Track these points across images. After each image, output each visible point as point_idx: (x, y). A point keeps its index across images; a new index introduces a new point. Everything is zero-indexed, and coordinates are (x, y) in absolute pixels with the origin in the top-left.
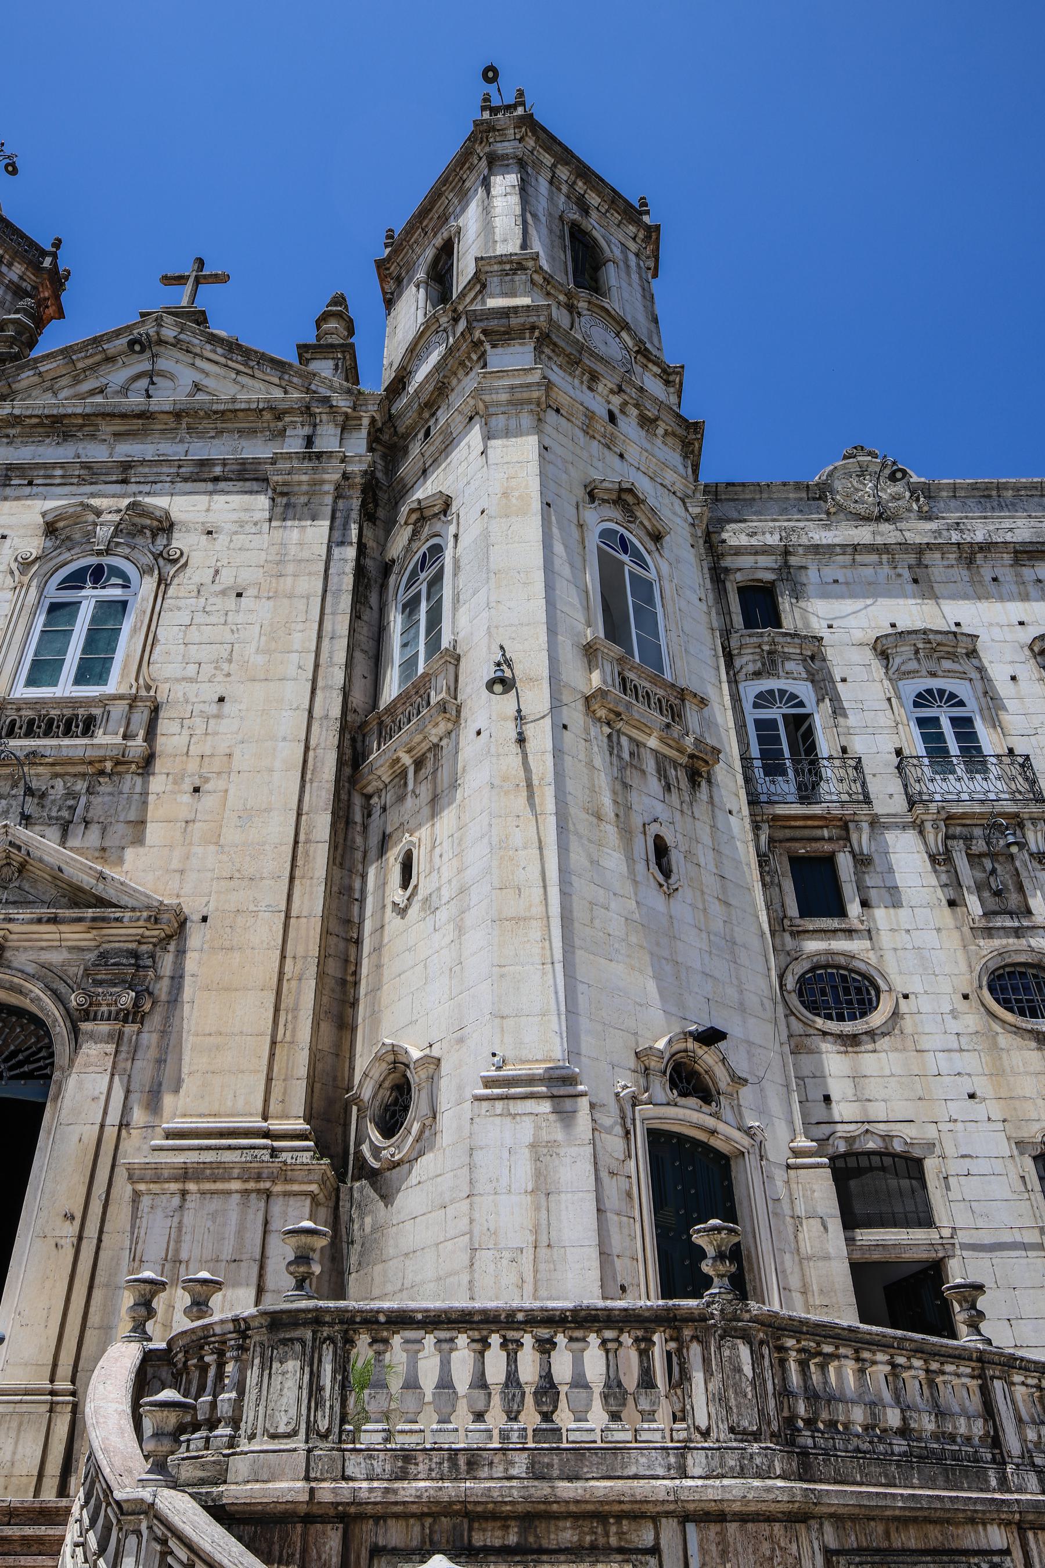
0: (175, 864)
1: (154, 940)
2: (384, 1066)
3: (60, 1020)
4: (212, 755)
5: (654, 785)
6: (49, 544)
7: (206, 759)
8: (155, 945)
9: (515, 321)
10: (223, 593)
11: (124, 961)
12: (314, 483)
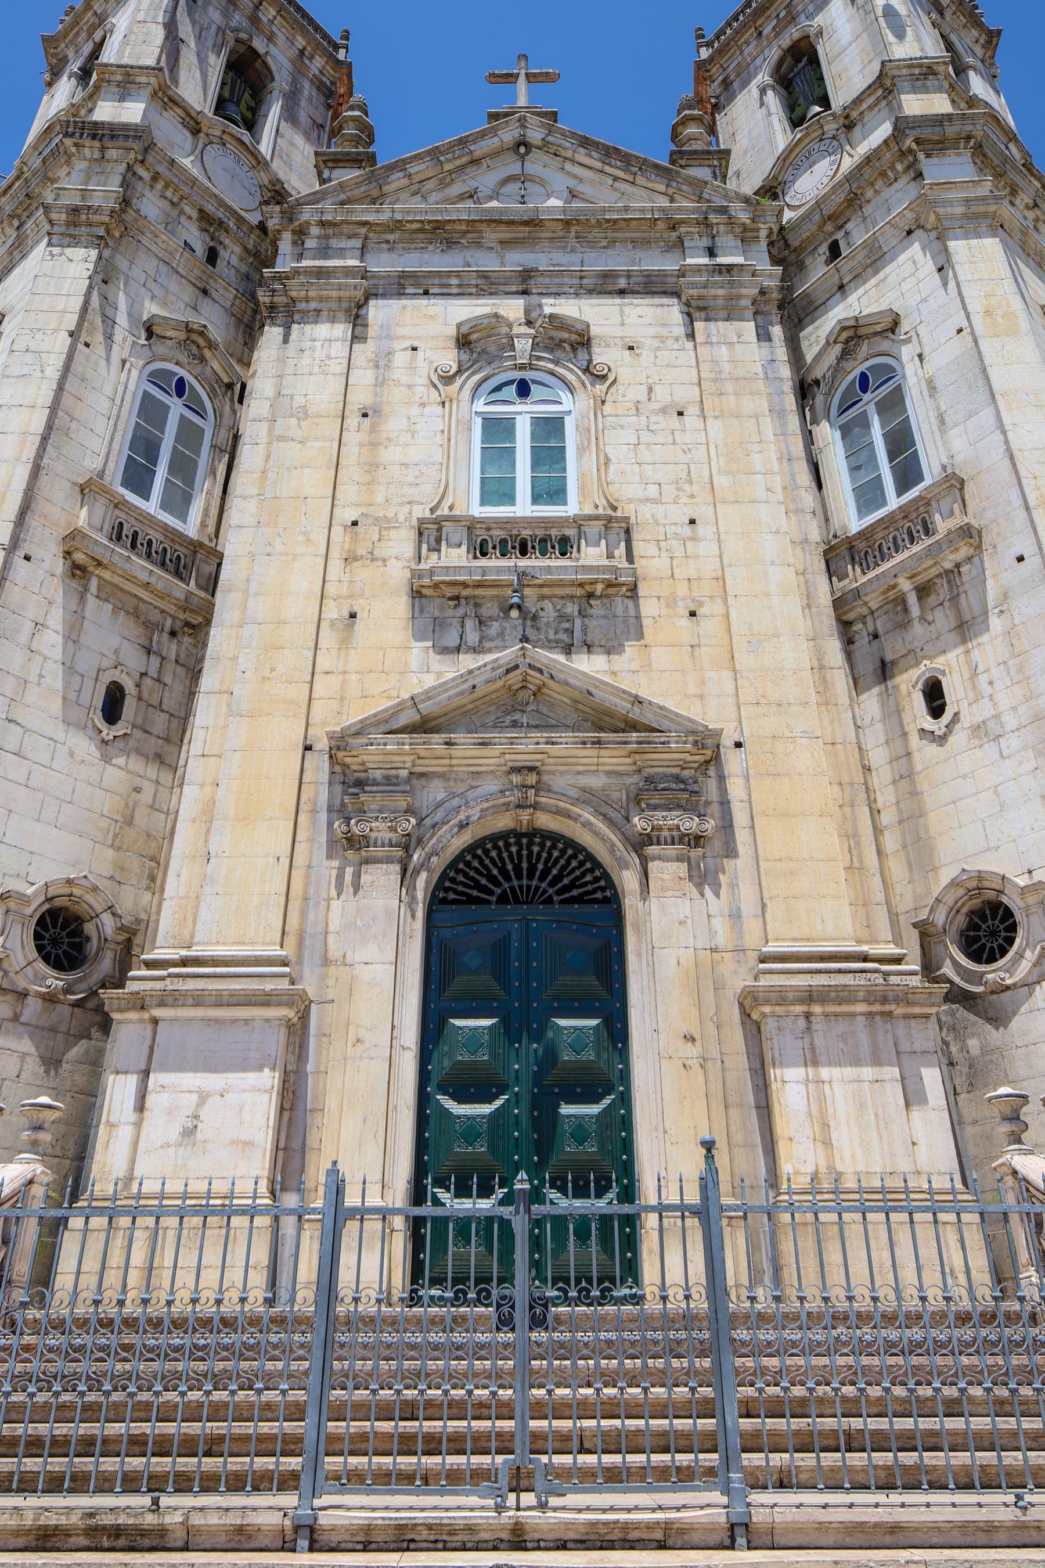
0: (692, 689)
1: (696, 765)
2: (961, 892)
3: (619, 844)
4: (699, 579)
6: (465, 357)
7: (694, 583)
8: (696, 770)
9: (951, 130)
10: (663, 411)
11: (674, 786)
12: (730, 298)
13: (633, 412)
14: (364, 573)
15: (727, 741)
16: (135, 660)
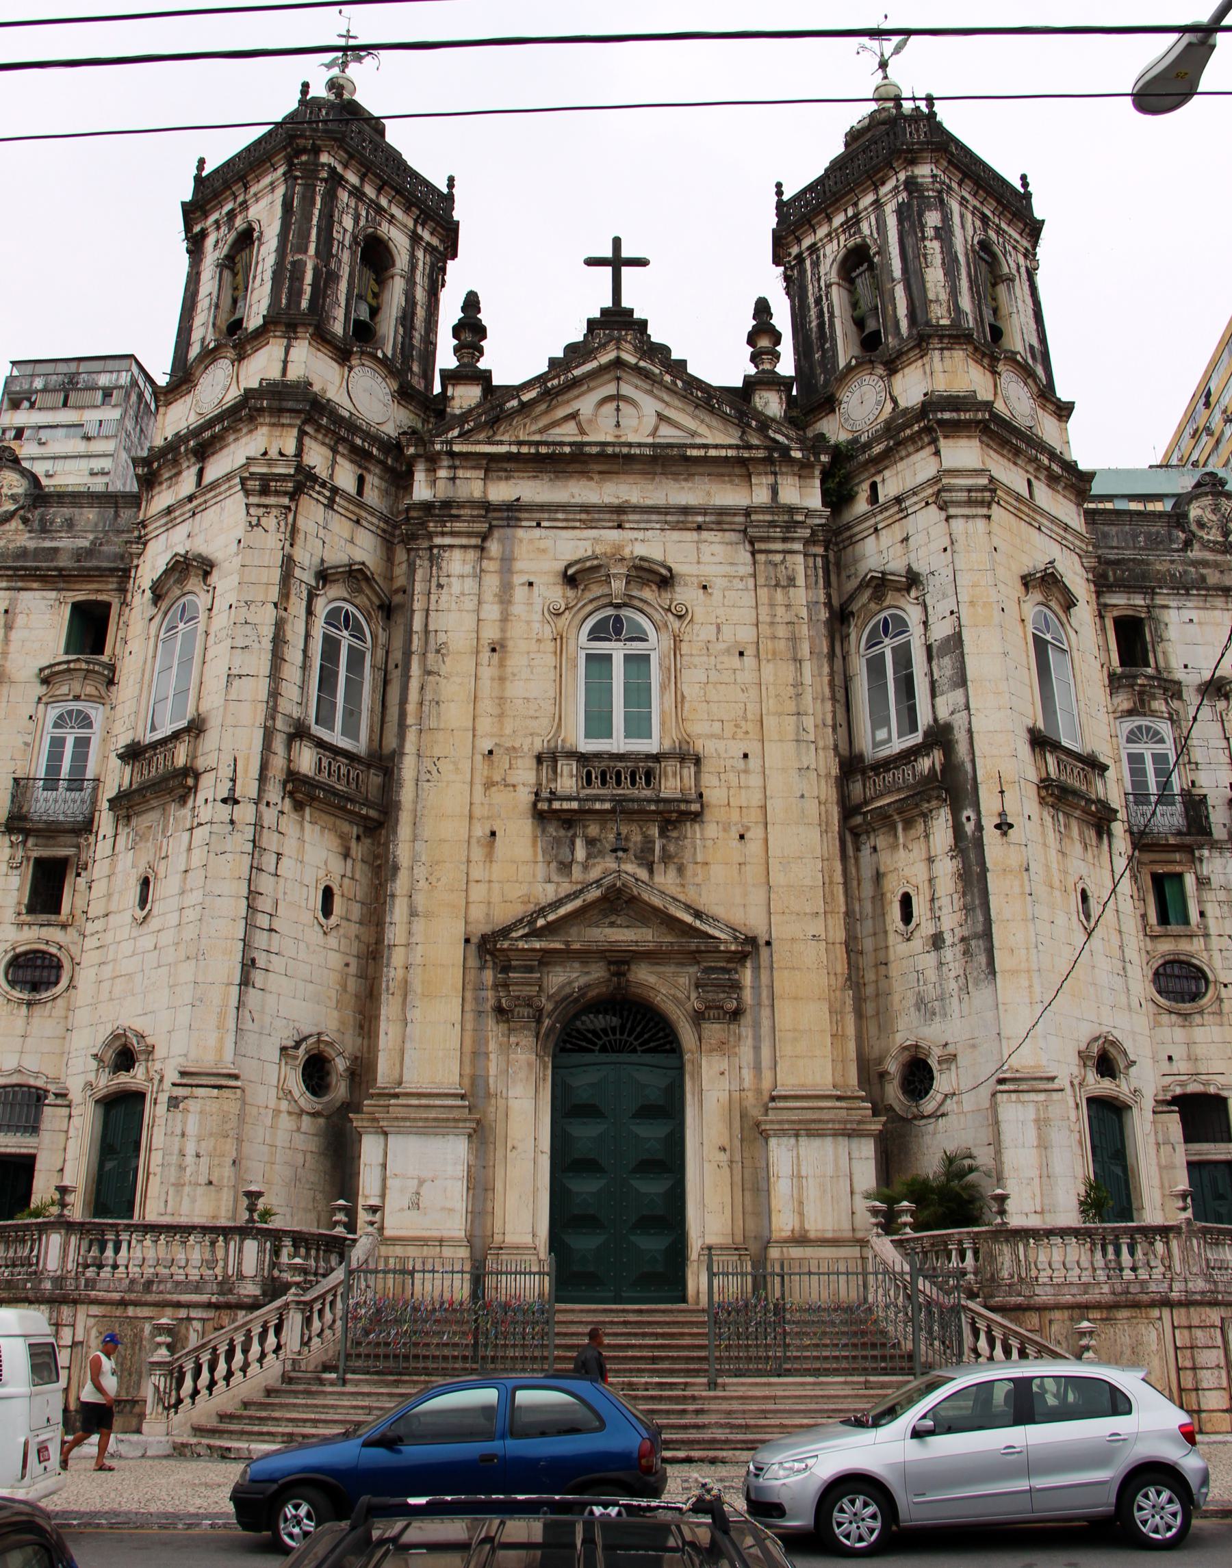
5: (1078, 847)
13: (705, 651)
14: (499, 797)
15: (762, 942)
16: (337, 866)
